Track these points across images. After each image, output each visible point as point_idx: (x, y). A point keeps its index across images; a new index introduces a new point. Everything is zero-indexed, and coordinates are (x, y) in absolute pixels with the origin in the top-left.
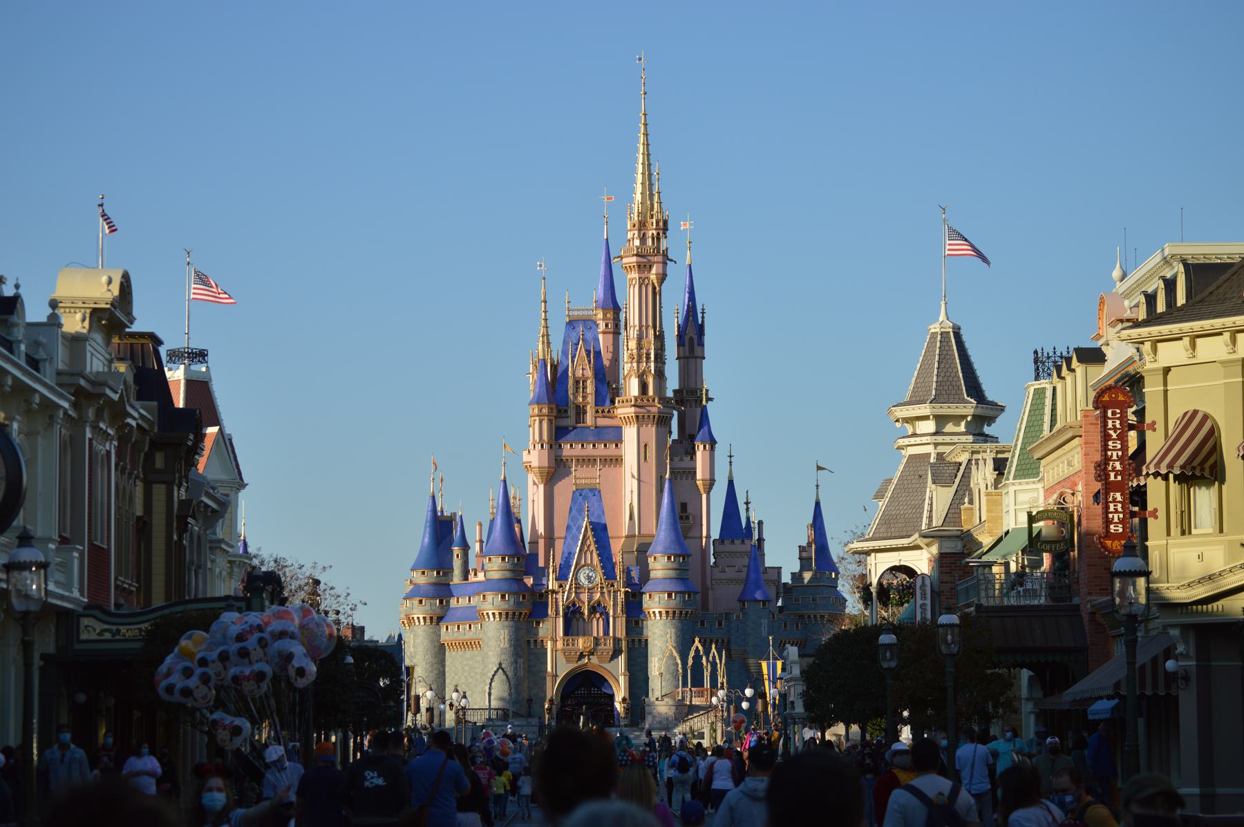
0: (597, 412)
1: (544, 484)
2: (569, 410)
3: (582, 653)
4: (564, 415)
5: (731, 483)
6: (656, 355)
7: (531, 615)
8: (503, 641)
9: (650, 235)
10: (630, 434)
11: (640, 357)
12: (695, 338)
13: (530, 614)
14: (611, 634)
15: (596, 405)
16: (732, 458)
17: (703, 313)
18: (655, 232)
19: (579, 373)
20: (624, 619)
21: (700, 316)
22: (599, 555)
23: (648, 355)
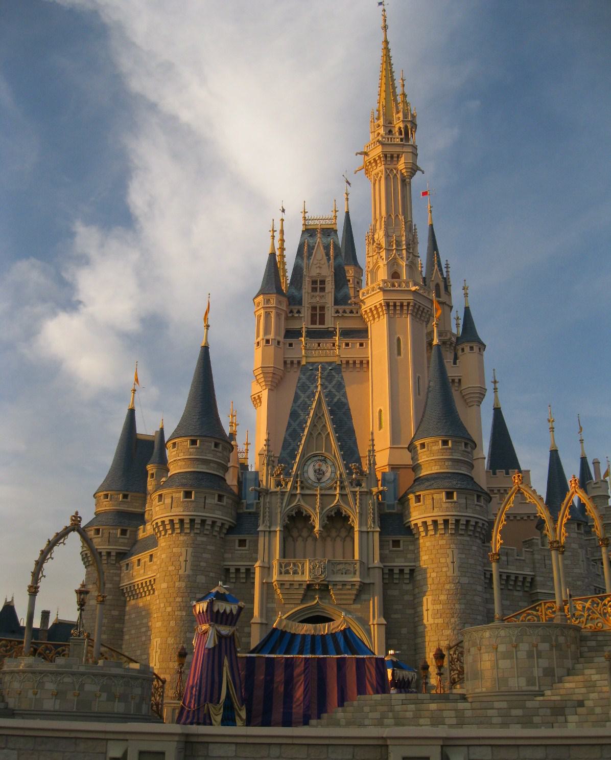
0: (337, 312)
1: (269, 389)
2: (302, 311)
3: (309, 586)
4: (297, 315)
5: (498, 412)
6: (408, 245)
7: (231, 530)
8: (183, 564)
9: (397, 129)
10: (379, 330)
11: (389, 243)
13: (230, 527)
14: (357, 557)
15: (334, 305)
16: (497, 384)
17: (447, 268)
18: (402, 125)
19: (314, 272)
20: (377, 536)
21: (444, 270)
22: (339, 439)
23: (398, 243)
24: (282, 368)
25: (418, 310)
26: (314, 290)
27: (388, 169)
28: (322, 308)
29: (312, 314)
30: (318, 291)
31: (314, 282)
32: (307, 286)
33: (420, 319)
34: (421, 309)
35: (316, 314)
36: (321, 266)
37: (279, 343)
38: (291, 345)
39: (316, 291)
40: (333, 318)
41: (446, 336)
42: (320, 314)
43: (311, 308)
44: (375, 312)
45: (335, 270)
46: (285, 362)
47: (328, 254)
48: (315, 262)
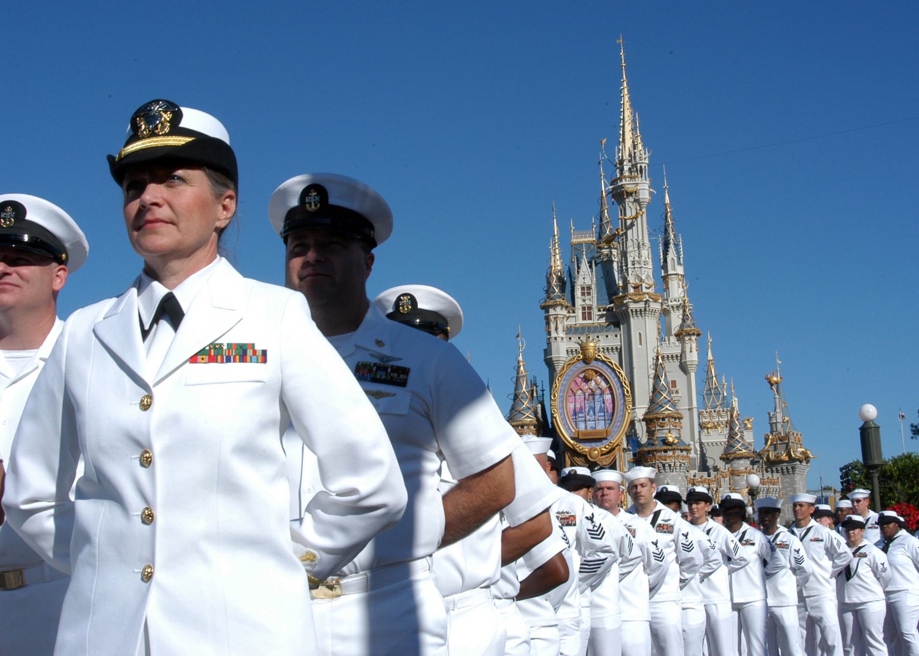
0: (599, 311)
2: (576, 311)
12: (676, 259)
24: (566, 356)
25: (652, 312)
26: (583, 294)
27: (629, 202)
28: (590, 308)
29: (583, 313)
30: (586, 294)
31: (583, 288)
32: (578, 293)
33: (654, 317)
34: (654, 311)
35: (585, 313)
36: (585, 276)
37: (562, 338)
38: (570, 339)
39: (584, 295)
40: (597, 316)
41: (679, 301)
42: (588, 312)
43: (581, 309)
44: (623, 314)
45: (596, 279)
46: (567, 350)
47: (591, 267)
48: (583, 273)
